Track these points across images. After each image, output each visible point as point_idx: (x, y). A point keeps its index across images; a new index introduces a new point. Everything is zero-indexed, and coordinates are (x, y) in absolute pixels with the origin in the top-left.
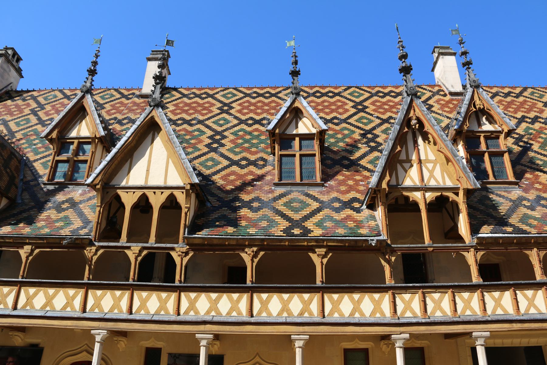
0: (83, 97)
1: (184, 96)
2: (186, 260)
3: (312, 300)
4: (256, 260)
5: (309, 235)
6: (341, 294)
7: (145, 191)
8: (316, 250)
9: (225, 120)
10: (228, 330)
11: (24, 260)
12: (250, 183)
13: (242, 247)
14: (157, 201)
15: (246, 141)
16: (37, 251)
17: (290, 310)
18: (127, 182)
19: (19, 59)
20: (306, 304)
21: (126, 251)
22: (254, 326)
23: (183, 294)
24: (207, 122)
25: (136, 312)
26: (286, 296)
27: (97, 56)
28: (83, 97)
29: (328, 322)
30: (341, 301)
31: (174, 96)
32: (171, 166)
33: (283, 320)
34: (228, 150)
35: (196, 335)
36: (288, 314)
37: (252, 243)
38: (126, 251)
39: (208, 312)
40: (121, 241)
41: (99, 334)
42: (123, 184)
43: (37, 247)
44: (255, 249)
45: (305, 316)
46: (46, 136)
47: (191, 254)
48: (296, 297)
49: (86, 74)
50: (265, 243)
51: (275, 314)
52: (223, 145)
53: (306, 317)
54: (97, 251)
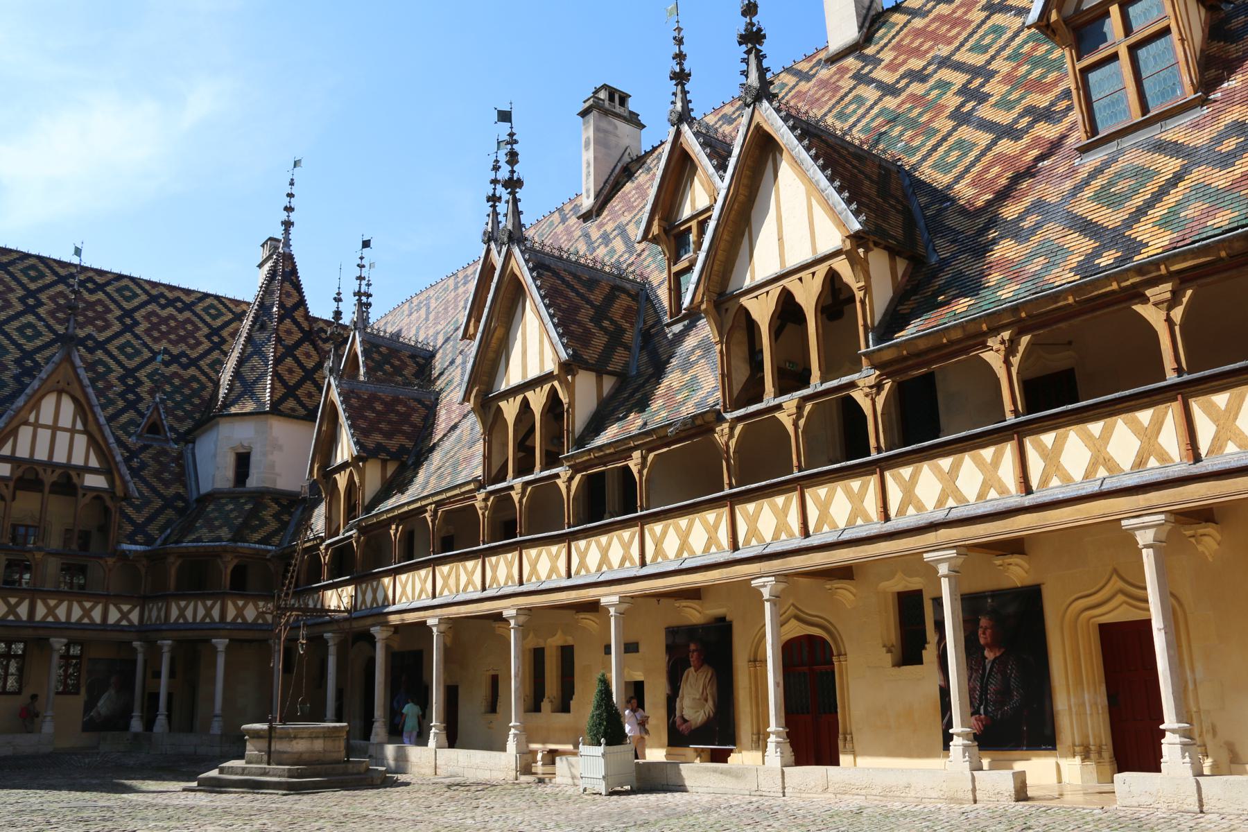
0: (678, 134)
1: (914, 13)
2: (880, 400)
3: (1162, 423)
4: (1015, 361)
5: (1136, 258)
6: (1236, 391)
7: (783, 282)
8: (1148, 293)
9: (994, 32)
10: (982, 533)
11: (637, 476)
12: (1030, 172)
13: (980, 340)
14: (807, 294)
15: (1036, 63)
16: (651, 456)
17: (1110, 459)
18: (752, 278)
19: (624, 99)
20: (1149, 436)
21: (777, 415)
22: (1035, 515)
23: (887, 474)
24: (956, 57)
25: (816, 530)
26: (1096, 428)
27: (680, 41)
28: (678, 134)
29: (1210, 469)
30: (1239, 408)
31: (895, 24)
32: (820, 214)
33: (1093, 488)
34: (995, 105)
35: (925, 555)
36: (1109, 470)
37: (995, 322)
38: (777, 415)
39: (940, 503)
40: (766, 398)
41: (764, 586)
42: (748, 283)
43: (650, 451)
44: (1006, 335)
45: (1149, 465)
46: (645, 238)
47: (888, 385)
48: (1120, 425)
49: (671, 86)
50: (1023, 315)
51: (1078, 475)
52: (982, 98)
53: (1154, 470)
54: (732, 429)
